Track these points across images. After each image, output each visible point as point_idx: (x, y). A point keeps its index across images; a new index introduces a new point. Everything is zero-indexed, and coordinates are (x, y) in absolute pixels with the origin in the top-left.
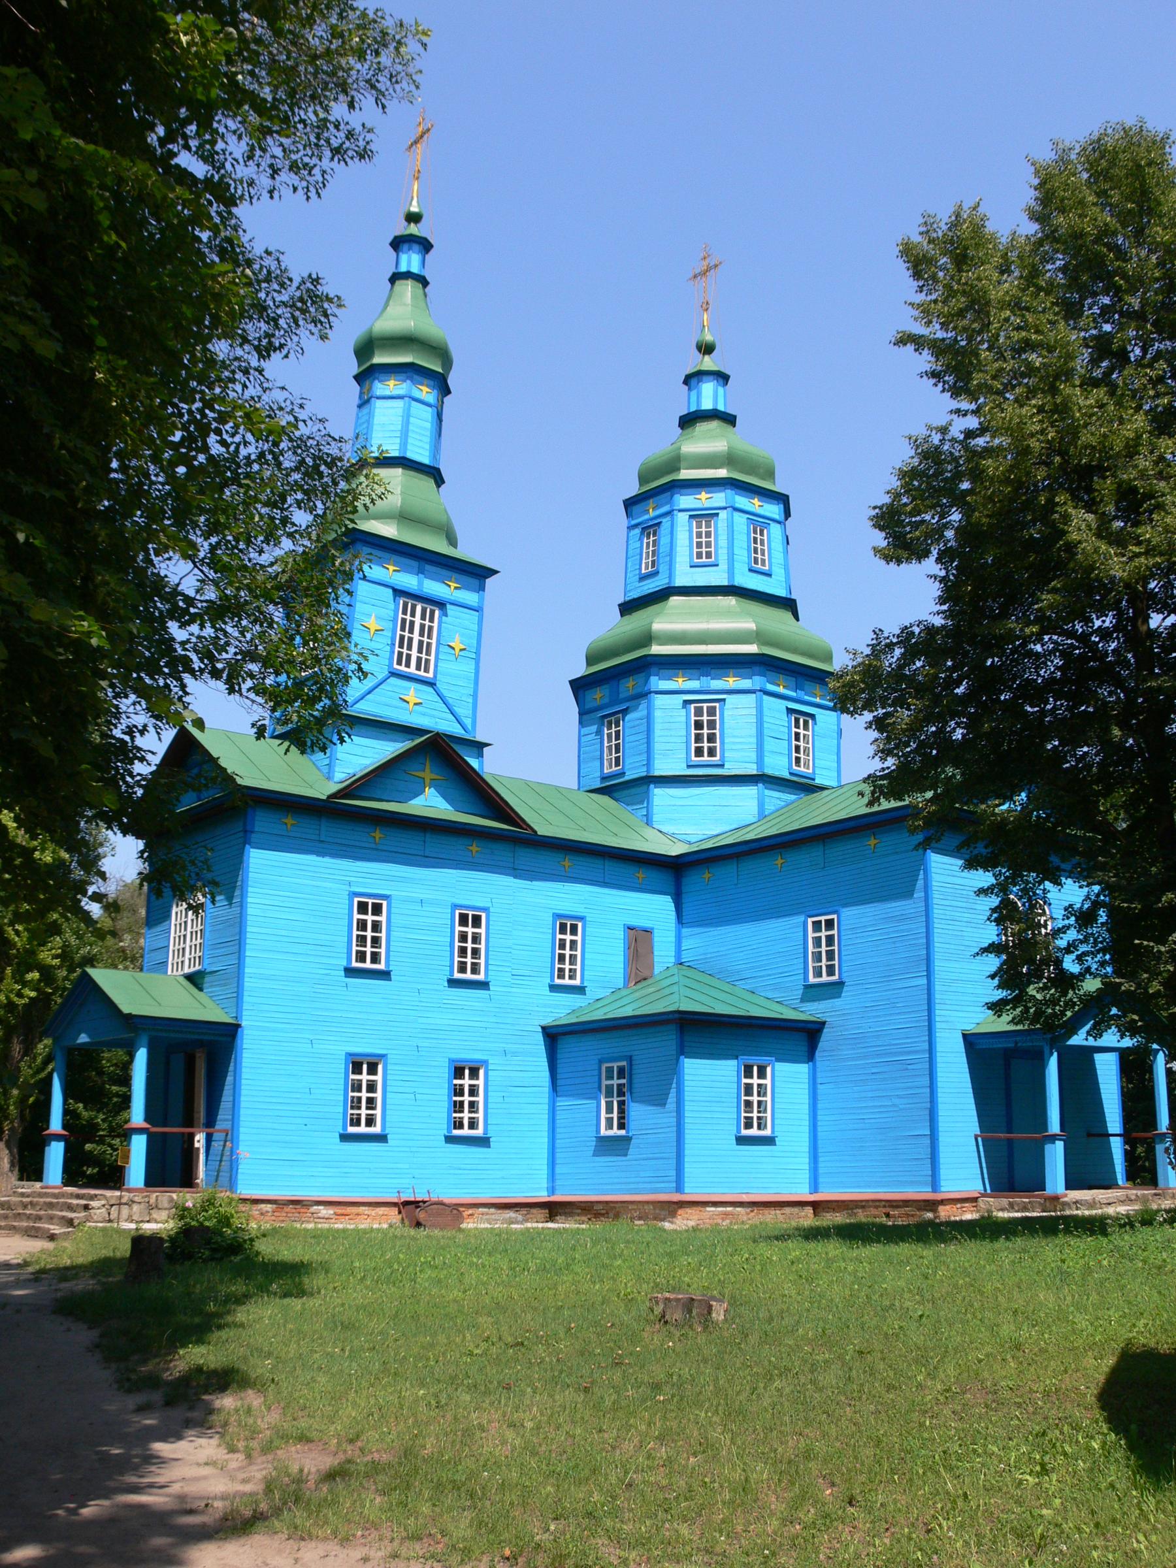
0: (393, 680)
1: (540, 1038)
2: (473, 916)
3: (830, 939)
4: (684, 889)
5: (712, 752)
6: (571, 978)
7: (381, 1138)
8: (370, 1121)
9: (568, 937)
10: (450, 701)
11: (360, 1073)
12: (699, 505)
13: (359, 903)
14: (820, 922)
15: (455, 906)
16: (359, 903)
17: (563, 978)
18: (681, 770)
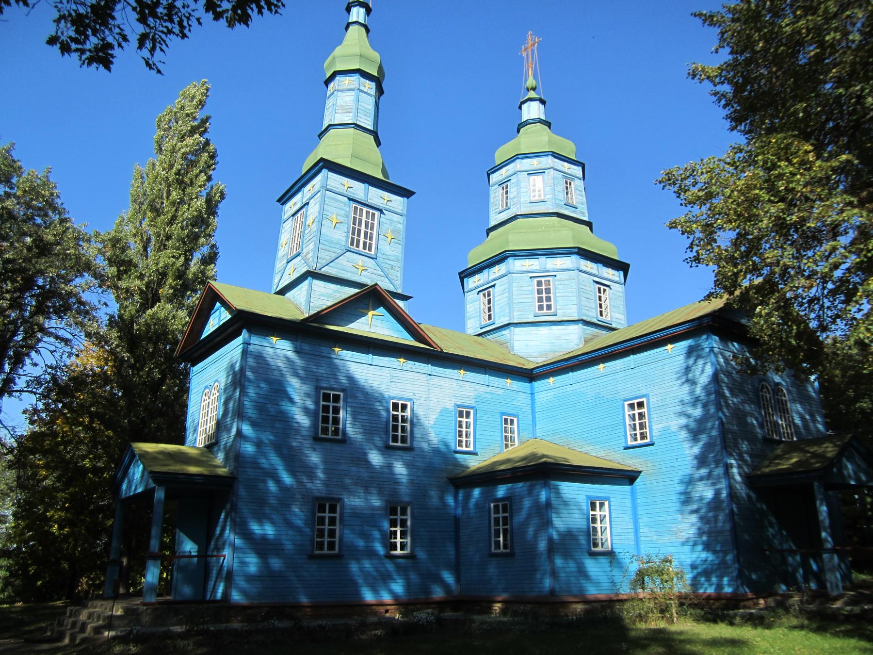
2: (402, 404)
3: (641, 416)
5: (549, 307)
6: (466, 446)
10: (386, 270)
11: (324, 512)
12: (533, 168)
13: (324, 394)
14: (634, 404)
16: (324, 394)
17: (462, 446)
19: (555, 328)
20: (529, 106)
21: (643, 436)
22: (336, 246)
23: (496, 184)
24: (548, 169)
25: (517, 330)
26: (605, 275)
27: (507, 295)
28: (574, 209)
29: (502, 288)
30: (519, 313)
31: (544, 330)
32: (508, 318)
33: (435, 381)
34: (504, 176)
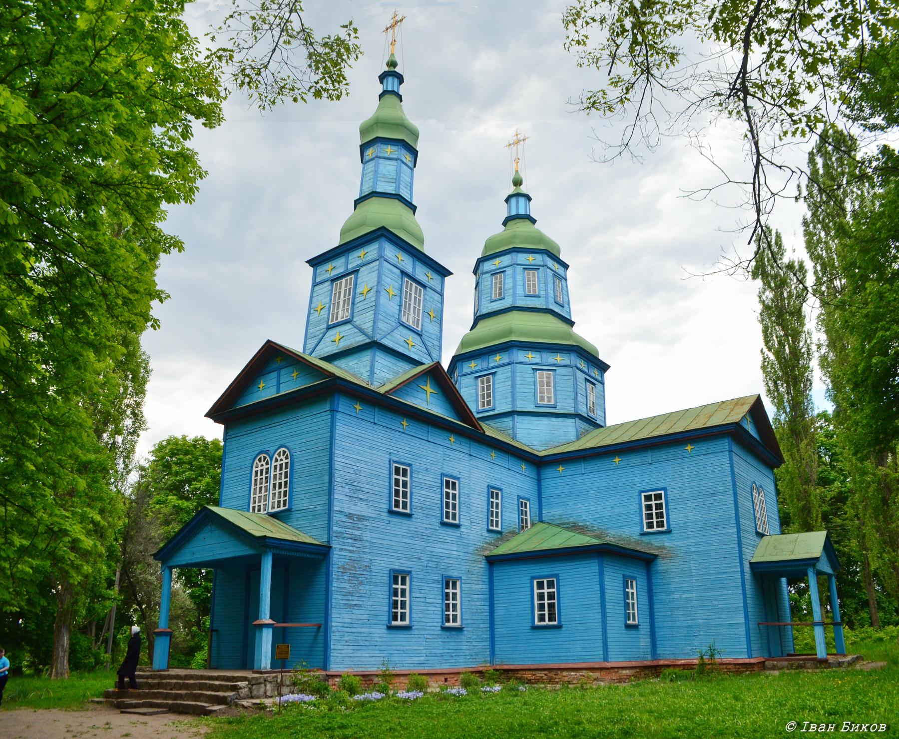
0: (401, 328)
1: (483, 565)
4: (543, 476)
7: (408, 628)
8: (403, 618)
9: (495, 501)
12: (527, 263)
15: (443, 475)
18: (532, 409)
19: (555, 421)
20: (517, 202)
21: (660, 524)
22: (391, 319)
23: (487, 272)
24: (543, 266)
25: (518, 419)
26: (593, 375)
27: (510, 383)
28: (561, 308)
29: (505, 376)
30: (522, 402)
31: (545, 421)
32: (511, 406)
33: (475, 462)
34: (498, 266)
